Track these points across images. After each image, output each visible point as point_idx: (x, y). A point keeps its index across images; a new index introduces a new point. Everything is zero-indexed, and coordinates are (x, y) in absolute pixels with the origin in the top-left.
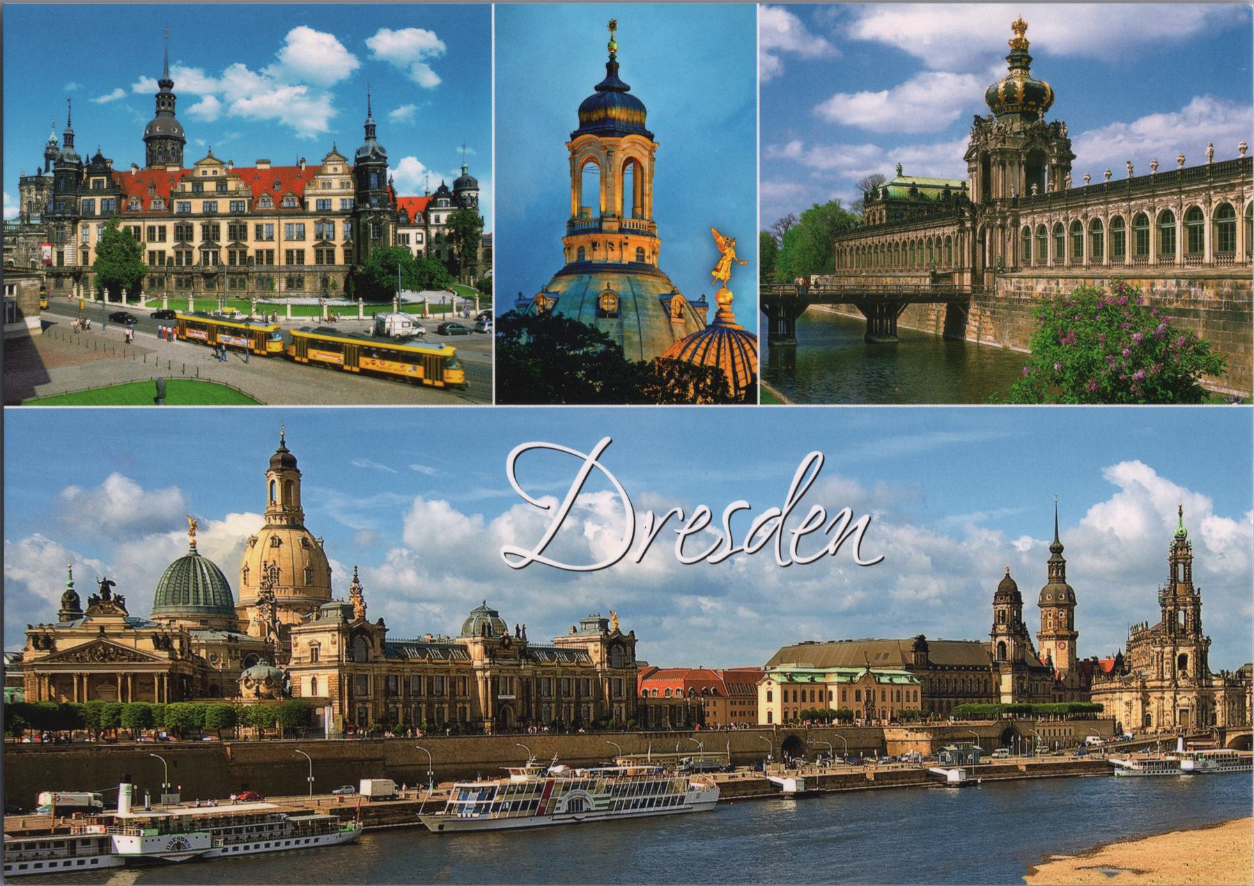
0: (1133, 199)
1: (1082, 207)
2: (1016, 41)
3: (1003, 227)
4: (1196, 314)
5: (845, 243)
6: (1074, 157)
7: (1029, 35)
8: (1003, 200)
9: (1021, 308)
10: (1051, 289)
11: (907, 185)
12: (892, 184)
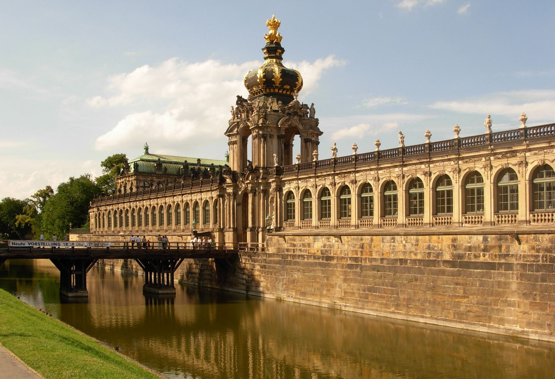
0: (406, 166)
1: (350, 172)
2: (270, 36)
3: (266, 192)
4: (509, 267)
5: (103, 208)
6: (321, 133)
7: (280, 31)
8: (264, 168)
9: (296, 263)
10: (330, 246)
11: (154, 161)
12: (142, 160)
